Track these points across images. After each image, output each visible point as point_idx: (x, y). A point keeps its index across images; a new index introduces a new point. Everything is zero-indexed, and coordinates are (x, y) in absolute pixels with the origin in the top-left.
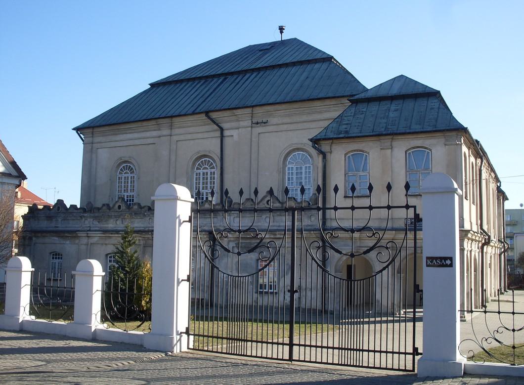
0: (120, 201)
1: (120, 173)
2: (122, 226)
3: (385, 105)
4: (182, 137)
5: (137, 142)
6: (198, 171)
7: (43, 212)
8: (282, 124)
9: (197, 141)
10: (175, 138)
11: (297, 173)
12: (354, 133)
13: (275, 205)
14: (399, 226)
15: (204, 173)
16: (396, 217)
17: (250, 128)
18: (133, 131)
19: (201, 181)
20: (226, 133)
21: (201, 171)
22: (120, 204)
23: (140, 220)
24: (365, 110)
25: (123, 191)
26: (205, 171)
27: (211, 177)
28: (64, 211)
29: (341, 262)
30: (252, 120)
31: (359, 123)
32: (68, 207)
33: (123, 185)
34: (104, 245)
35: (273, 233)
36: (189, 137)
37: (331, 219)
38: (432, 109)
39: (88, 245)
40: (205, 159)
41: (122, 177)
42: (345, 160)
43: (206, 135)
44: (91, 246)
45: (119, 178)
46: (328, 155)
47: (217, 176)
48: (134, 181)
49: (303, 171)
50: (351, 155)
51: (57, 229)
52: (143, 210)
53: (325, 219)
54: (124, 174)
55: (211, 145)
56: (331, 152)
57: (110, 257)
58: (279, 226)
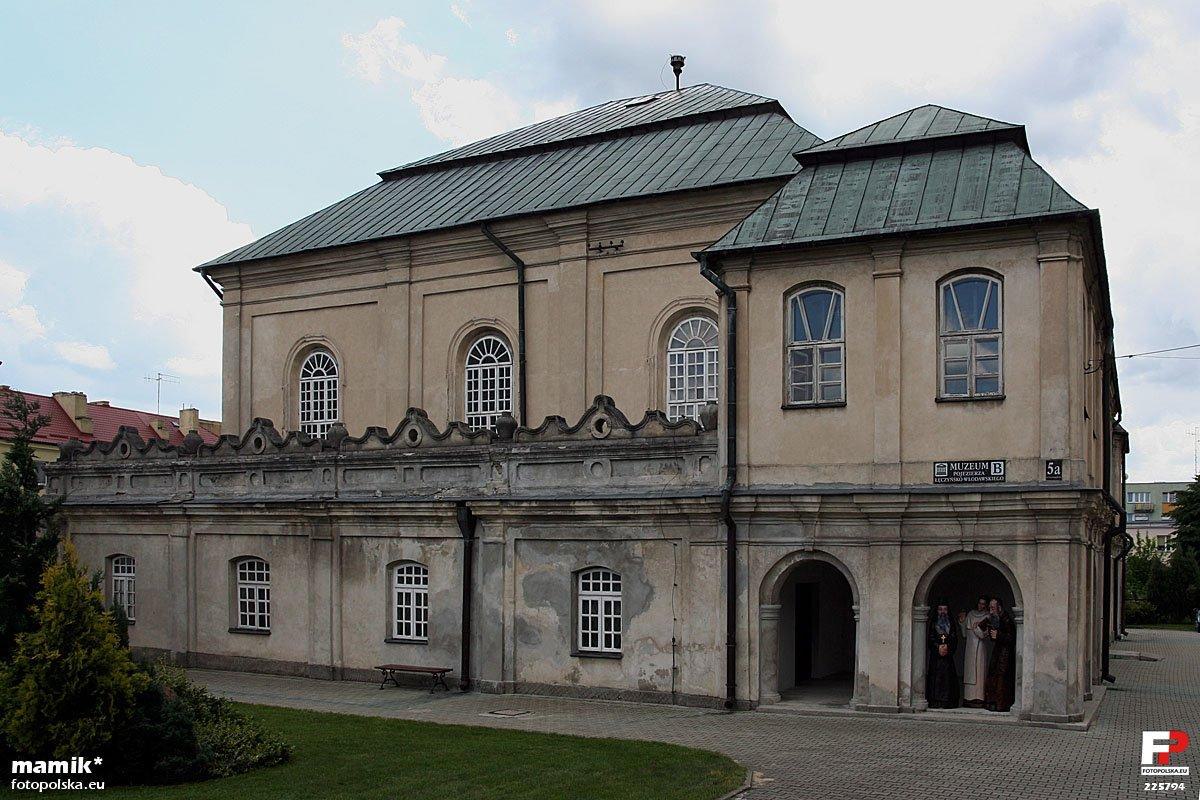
3: (883, 171)
4: (435, 287)
5: (337, 300)
10: (419, 289)
13: (615, 432)
15: (485, 372)
19: (480, 390)
21: (480, 367)
25: (312, 416)
26: (488, 366)
27: (501, 381)
34: (225, 537)
36: (451, 285)
38: (1002, 171)
39: (188, 537)
40: (488, 337)
43: (487, 280)
44: (195, 539)
45: (303, 384)
47: (514, 377)
48: (335, 392)
53: (735, 466)
55: (500, 307)
58: (625, 487)
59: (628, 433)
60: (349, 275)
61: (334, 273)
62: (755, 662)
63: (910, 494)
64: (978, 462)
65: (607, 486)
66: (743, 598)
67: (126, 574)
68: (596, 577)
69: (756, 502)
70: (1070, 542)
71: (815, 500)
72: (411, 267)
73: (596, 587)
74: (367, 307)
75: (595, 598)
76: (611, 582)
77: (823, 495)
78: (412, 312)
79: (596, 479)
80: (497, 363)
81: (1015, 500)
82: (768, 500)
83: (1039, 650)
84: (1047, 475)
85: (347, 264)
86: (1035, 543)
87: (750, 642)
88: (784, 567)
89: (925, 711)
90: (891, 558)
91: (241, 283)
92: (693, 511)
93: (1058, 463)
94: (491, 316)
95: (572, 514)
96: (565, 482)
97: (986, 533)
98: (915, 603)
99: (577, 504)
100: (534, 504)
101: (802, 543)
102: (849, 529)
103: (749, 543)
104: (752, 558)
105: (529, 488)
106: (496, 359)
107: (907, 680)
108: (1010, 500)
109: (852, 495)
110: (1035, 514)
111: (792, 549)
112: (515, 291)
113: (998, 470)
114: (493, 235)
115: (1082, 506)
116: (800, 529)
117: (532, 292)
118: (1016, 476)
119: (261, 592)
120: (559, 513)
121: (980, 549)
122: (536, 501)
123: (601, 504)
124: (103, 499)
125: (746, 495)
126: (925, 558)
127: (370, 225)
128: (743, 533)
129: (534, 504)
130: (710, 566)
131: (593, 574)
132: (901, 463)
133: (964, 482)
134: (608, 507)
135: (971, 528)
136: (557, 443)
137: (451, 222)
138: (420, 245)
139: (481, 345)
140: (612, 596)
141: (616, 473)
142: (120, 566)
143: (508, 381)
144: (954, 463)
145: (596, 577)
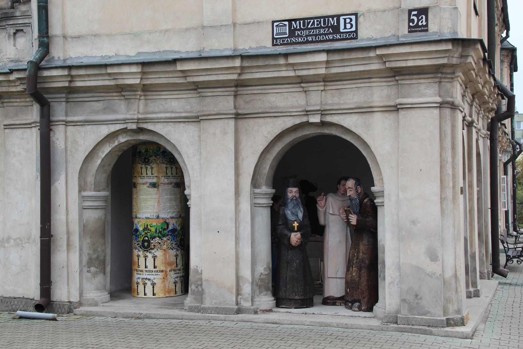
14: (254, 45)
16: (249, 20)
29: (99, 161)
37: (65, 37)
62: (75, 258)
63: (243, 57)
64: (324, 17)
66: (59, 186)
69: (72, 76)
70: (441, 105)
71: (134, 69)
77: (144, 64)
81: (370, 58)
82: (82, 72)
83: (403, 236)
84: (410, 27)
86: (396, 109)
87: (68, 233)
88: (107, 149)
89: (270, 311)
90: (225, 133)
93: (423, 11)
97: (336, 100)
98: (255, 184)
101: (125, 120)
102: (179, 104)
103: (67, 123)
104: (70, 140)
107: (246, 273)
108: (363, 59)
109: (174, 61)
110: (397, 74)
113: (348, 26)
115: (455, 61)
118: (369, 32)
121: (329, 119)
125: (56, 68)
126: (261, 135)
128: (59, 112)
132: (234, 25)
133: (307, 42)
135: (317, 98)
144: (295, 20)
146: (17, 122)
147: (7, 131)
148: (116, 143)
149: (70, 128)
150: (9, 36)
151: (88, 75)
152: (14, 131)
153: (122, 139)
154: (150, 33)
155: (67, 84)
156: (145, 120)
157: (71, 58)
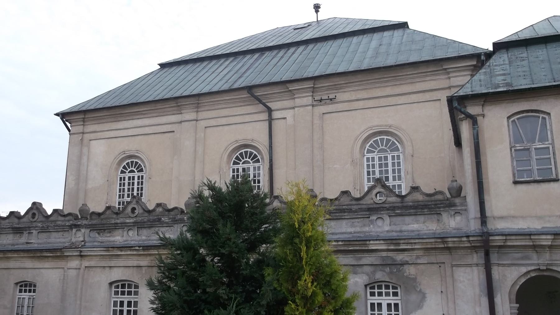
0: (134, 202)
1: (122, 172)
2: (137, 238)
6: (236, 167)
7: (7, 221)
8: (357, 100)
9: (234, 126)
10: (203, 124)
11: (380, 166)
12: (521, 85)
17: (310, 107)
18: (142, 116)
20: (276, 115)
22: (135, 206)
23: (167, 228)
24: (525, 55)
28: (41, 218)
29: (518, 287)
30: (312, 96)
31: (524, 72)
32: (49, 212)
33: (126, 187)
34: (107, 269)
35: (394, 242)
36: (224, 121)
37: (494, 218)
40: (246, 150)
41: (124, 178)
42: (508, 126)
43: (247, 118)
46: (479, 119)
49: (390, 161)
50: (518, 119)
51: (29, 246)
52: (172, 213)
54: (129, 172)
56: (483, 116)
57: (117, 287)
58: (401, 231)
59: (399, 200)
60: (157, 116)
61: (146, 116)
65: (388, 231)
66: (498, 300)
67: (27, 294)
68: (380, 287)
71: (549, 237)
72: (197, 112)
73: (380, 294)
74: (167, 134)
75: (379, 302)
76: (391, 291)
78: (197, 136)
79: (379, 227)
80: (252, 164)
85: (156, 111)
88: (523, 280)
91: (84, 122)
92: (456, 245)
94: (249, 137)
95: (366, 248)
96: (358, 229)
99: (371, 242)
100: (340, 243)
103: (499, 265)
105: (333, 234)
106: (251, 162)
111: (530, 268)
112: (266, 124)
114: (253, 93)
116: (535, 256)
117: (275, 124)
119: (129, 304)
120: (358, 248)
122: (342, 241)
123: (389, 242)
124: (16, 247)
125: (499, 235)
127: (168, 90)
128: (494, 258)
129: (340, 243)
130: (468, 279)
131: (378, 286)
134: (393, 244)
136: (350, 207)
137: (226, 87)
138: (204, 100)
139: (241, 154)
140: (392, 300)
141: (392, 223)
142: (23, 288)
143: (259, 174)
145: (380, 287)
146: (462, 263)
147: (454, 268)
148: (529, 277)
149: (500, 268)
150: (451, 216)
151: (516, 239)
152: (459, 268)
153: (533, 274)
154: (550, 217)
155: (502, 244)
156: (551, 265)
157: (498, 229)
